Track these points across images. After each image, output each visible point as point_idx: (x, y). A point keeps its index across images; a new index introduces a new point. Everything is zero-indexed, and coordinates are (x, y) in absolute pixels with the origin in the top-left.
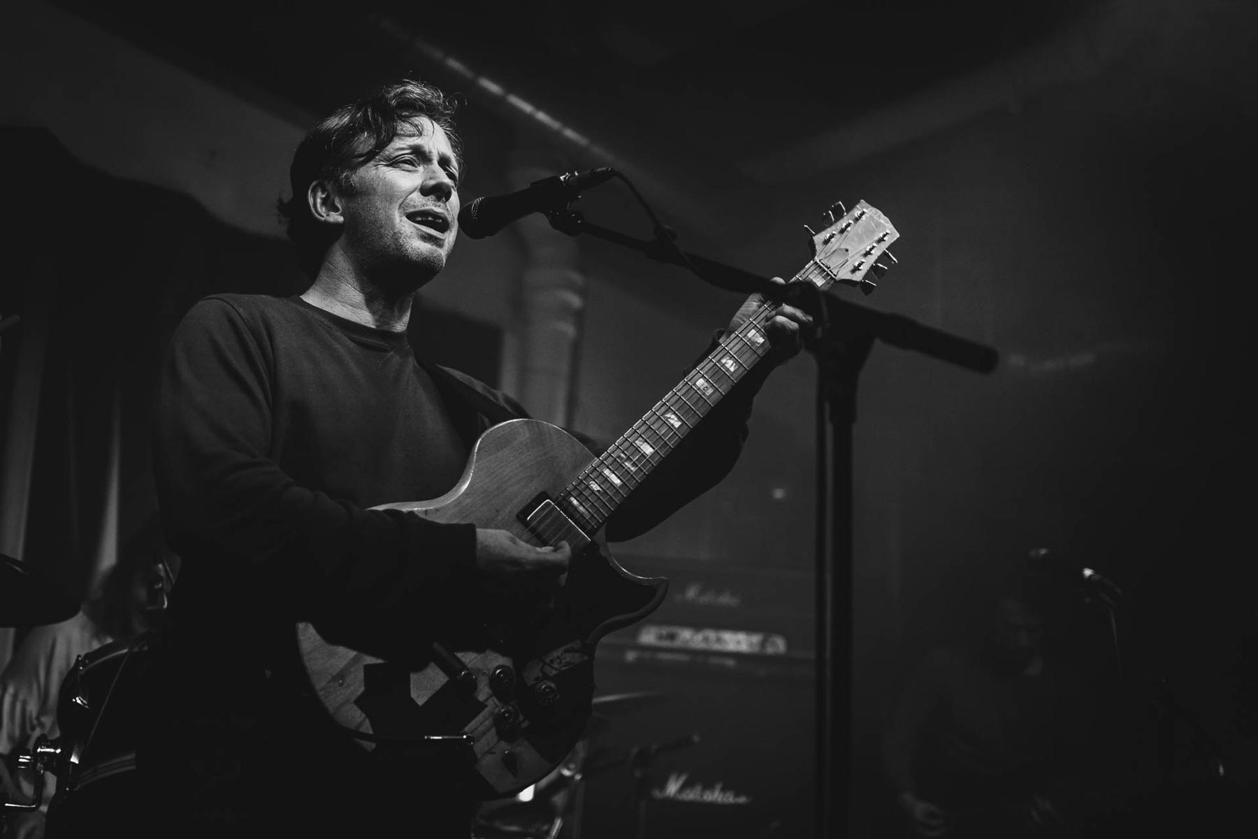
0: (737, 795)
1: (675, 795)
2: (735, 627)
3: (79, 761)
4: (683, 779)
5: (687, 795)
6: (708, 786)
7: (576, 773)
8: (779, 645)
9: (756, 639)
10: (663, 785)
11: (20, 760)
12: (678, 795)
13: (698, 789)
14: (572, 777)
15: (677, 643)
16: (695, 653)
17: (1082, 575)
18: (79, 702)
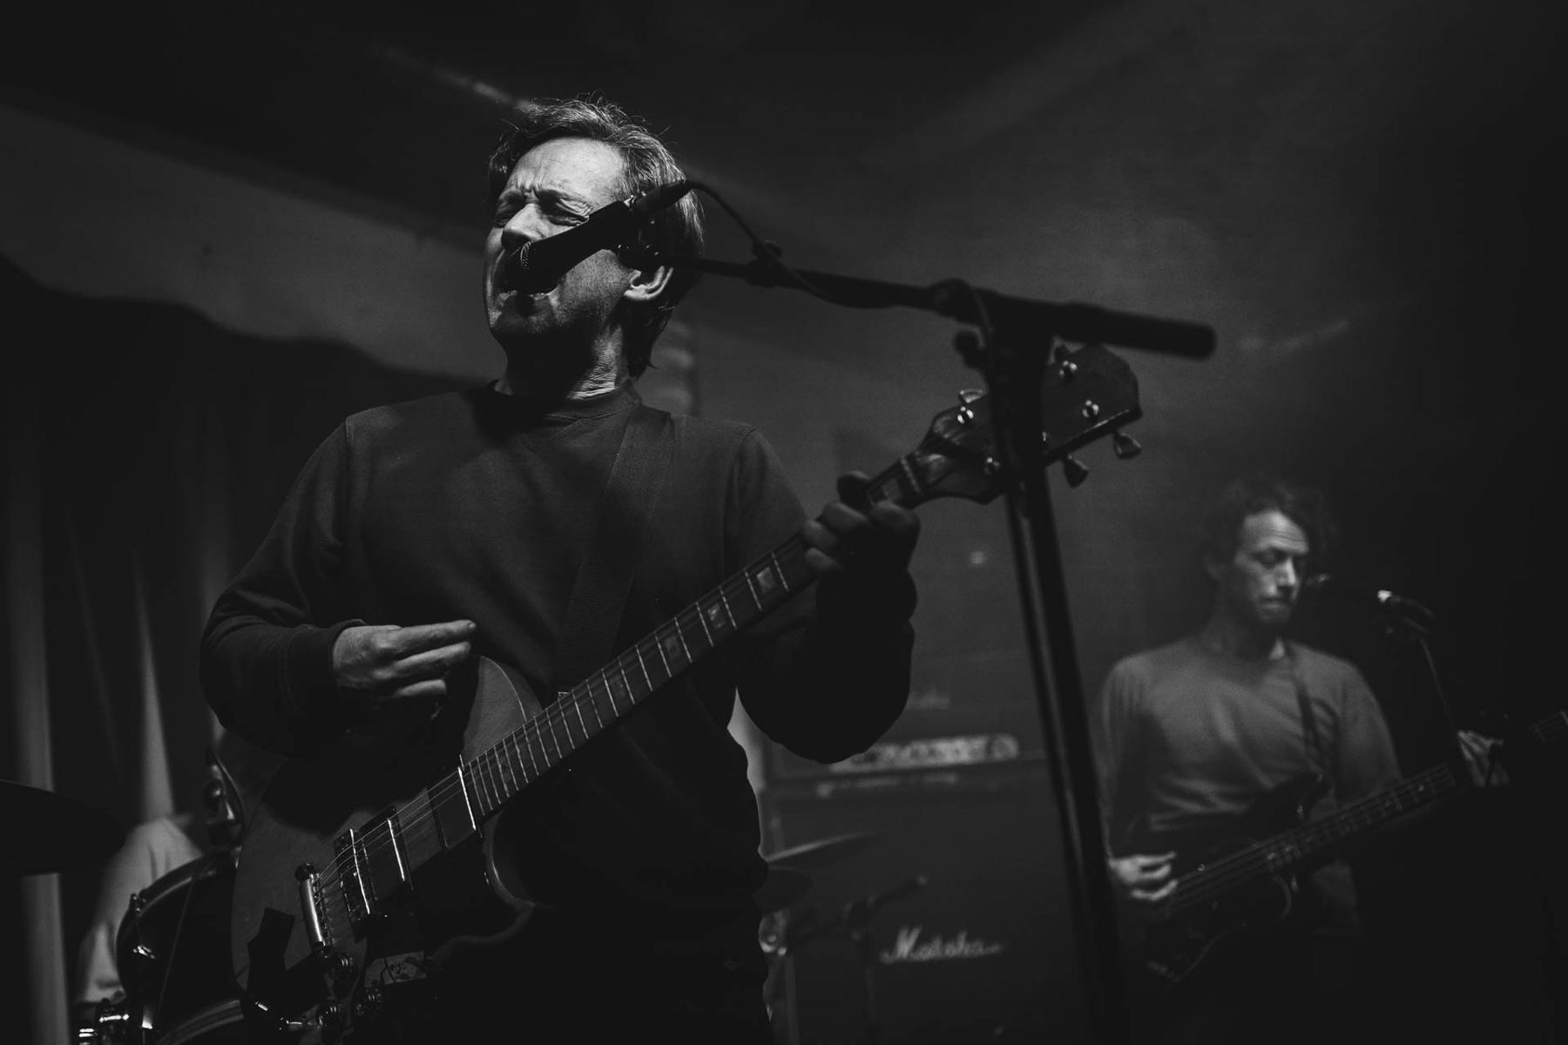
0: (987, 943)
1: (909, 954)
2: (950, 733)
3: (153, 1026)
4: (915, 934)
5: (924, 952)
6: (950, 937)
7: (779, 947)
8: (1008, 747)
9: (979, 743)
10: (892, 945)
11: (81, 1035)
12: (912, 955)
13: (937, 943)
14: (775, 953)
15: (881, 765)
16: (904, 773)
17: (1378, 600)
18: (142, 952)
